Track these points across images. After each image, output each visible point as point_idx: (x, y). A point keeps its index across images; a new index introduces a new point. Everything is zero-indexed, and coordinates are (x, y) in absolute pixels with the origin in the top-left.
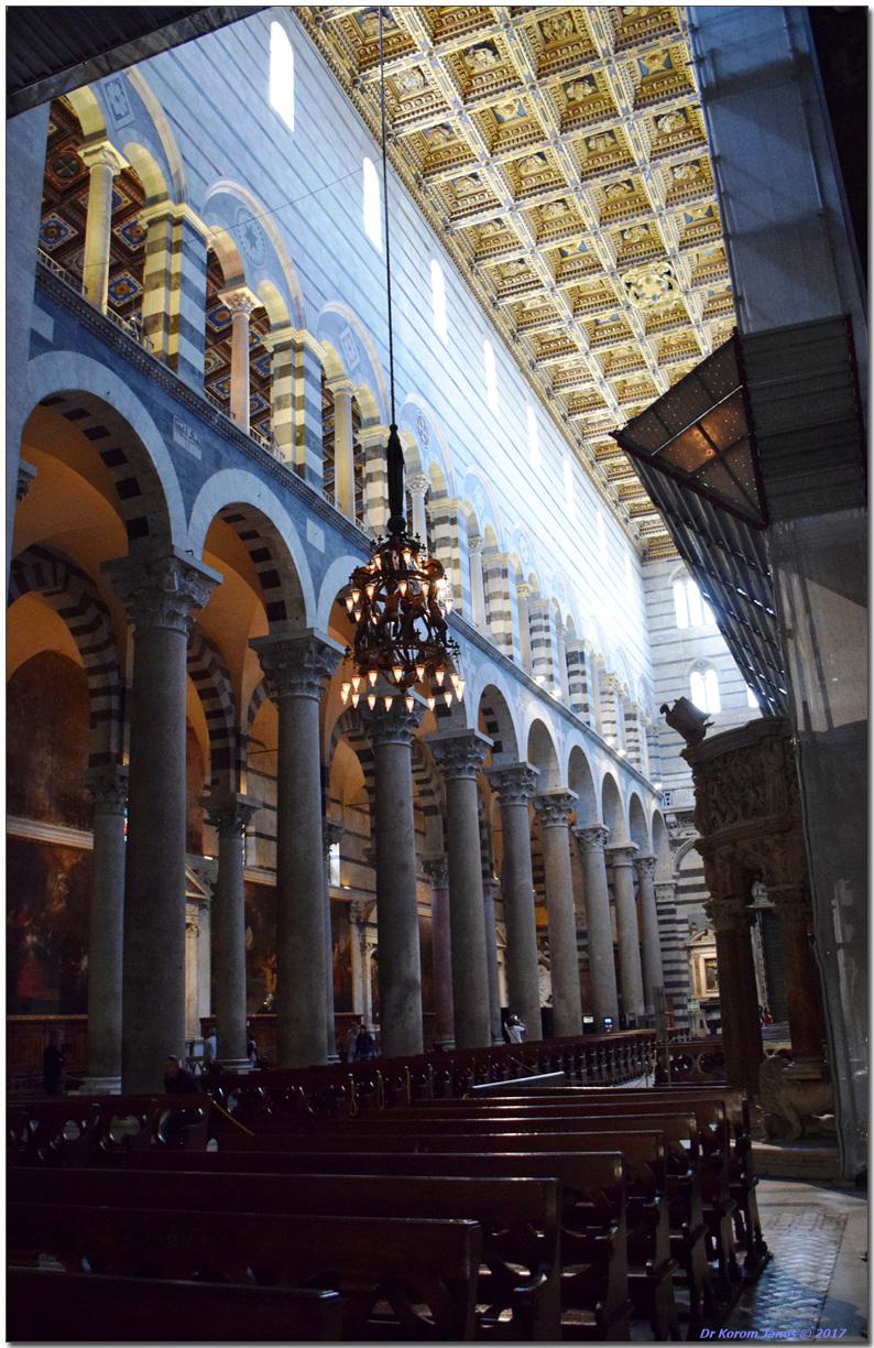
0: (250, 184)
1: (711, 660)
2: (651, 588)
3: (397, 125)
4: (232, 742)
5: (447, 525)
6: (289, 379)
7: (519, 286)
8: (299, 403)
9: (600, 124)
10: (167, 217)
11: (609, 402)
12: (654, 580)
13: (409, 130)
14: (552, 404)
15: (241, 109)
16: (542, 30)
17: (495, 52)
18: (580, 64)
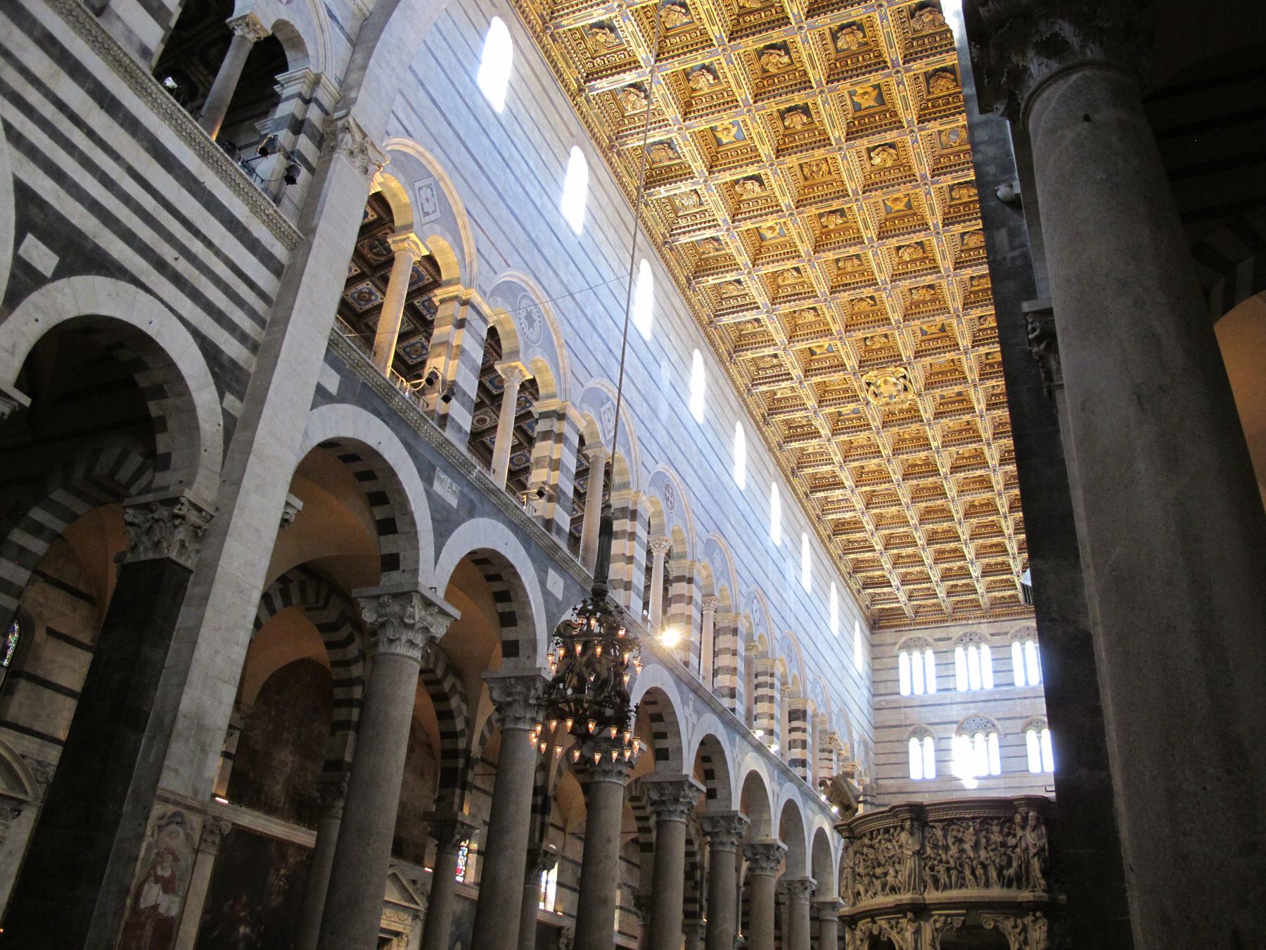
0: (535, 275)
1: (930, 728)
2: (879, 655)
3: (674, 235)
4: (461, 763)
5: (684, 584)
6: (549, 443)
7: (772, 377)
8: (556, 465)
9: (848, 249)
10: (456, 298)
11: (847, 484)
12: (881, 648)
13: (684, 239)
14: (795, 482)
15: (535, 212)
16: (802, 170)
17: (761, 184)
18: (833, 199)
